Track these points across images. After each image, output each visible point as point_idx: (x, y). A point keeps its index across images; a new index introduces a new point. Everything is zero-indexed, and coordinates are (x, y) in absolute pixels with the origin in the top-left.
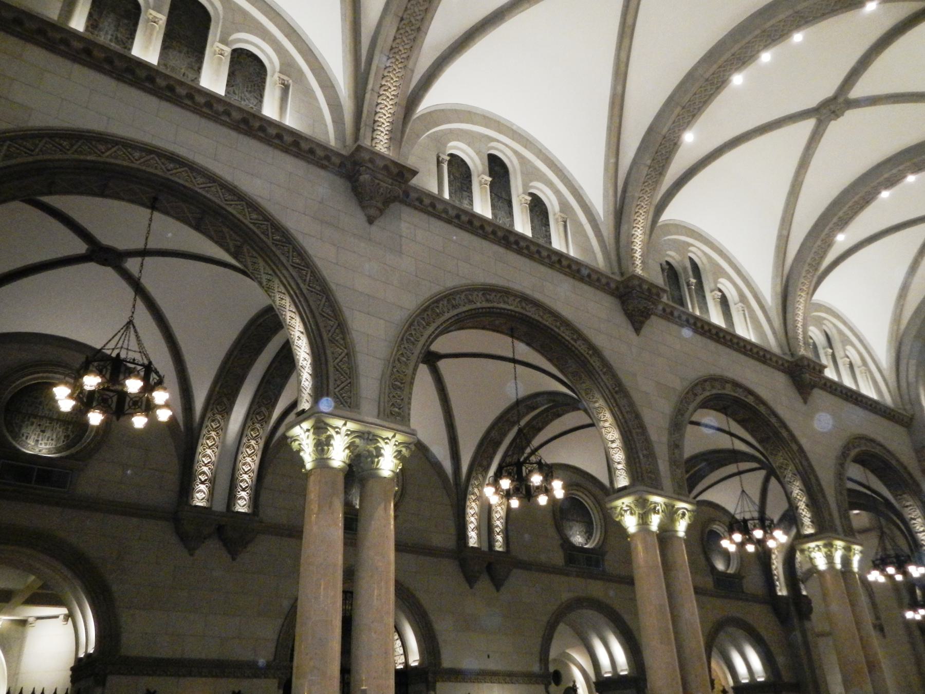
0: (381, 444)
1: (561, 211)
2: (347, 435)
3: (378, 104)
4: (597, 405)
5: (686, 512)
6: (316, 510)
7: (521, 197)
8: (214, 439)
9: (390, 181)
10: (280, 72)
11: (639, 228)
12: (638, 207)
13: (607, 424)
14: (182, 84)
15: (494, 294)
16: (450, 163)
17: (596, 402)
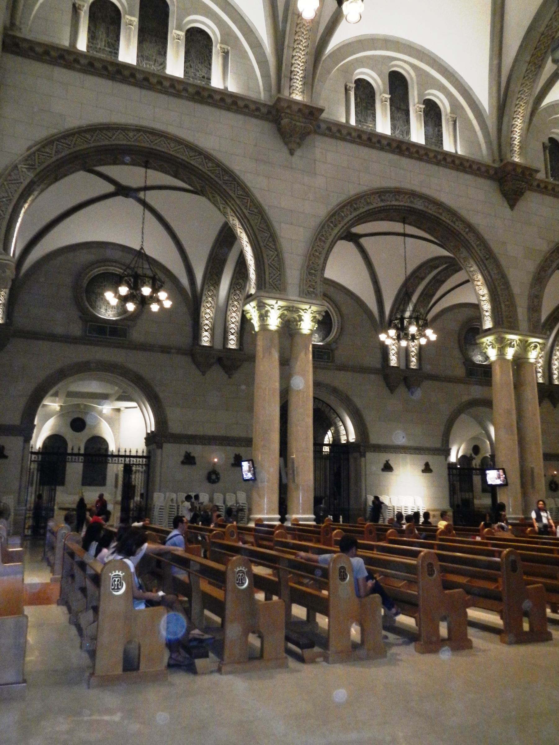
0: (302, 313)
1: (452, 112)
2: (279, 309)
3: (293, 57)
4: (472, 269)
5: (538, 345)
6: (261, 357)
7: (416, 107)
8: (211, 303)
9: (304, 120)
10: (221, 43)
11: (519, 118)
12: (519, 100)
13: (479, 283)
14: (154, 75)
15: (387, 195)
16: (356, 89)
17: (471, 267)
